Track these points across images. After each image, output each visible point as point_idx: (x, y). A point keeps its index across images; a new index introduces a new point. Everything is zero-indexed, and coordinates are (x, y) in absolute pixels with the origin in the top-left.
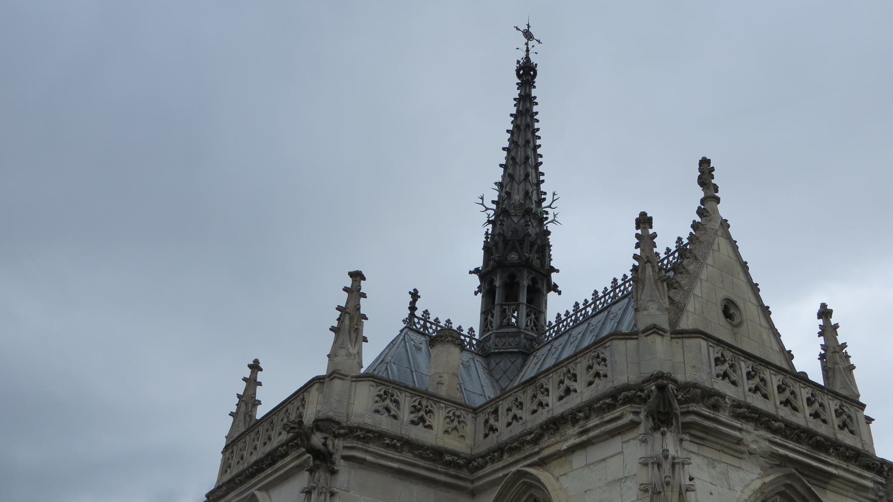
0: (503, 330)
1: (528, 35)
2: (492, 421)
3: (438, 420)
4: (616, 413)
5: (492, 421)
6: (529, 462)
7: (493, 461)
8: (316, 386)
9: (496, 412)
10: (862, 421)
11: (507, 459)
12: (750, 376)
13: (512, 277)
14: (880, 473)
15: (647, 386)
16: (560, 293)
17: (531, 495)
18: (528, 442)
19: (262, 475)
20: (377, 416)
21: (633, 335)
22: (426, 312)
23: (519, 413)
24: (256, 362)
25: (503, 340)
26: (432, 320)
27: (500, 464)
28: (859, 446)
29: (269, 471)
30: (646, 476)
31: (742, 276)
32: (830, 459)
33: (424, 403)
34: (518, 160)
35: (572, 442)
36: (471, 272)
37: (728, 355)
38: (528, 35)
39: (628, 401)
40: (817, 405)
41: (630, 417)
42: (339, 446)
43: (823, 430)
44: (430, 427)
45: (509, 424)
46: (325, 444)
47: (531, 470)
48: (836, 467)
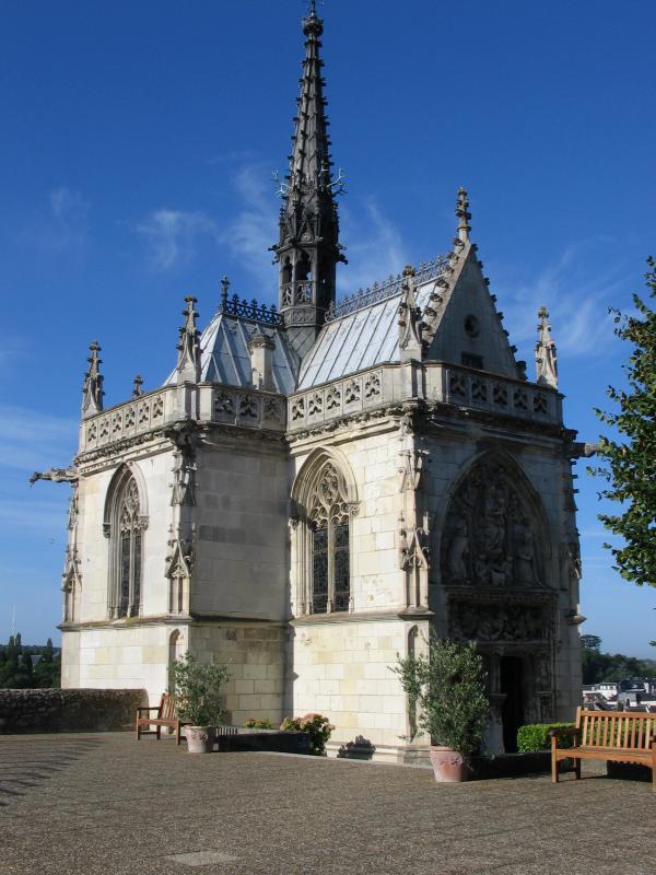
2: (298, 409)
3: (260, 411)
6: (327, 442)
9: (301, 401)
10: (554, 398)
11: (312, 438)
12: (474, 386)
14: (560, 437)
16: (346, 262)
17: (329, 463)
20: (219, 414)
22: (236, 296)
23: (319, 407)
25: (301, 315)
28: (548, 421)
33: (249, 399)
35: (356, 434)
36: (270, 250)
37: (460, 375)
40: (521, 398)
41: (392, 424)
43: (523, 415)
44: (254, 416)
45: (312, 413)
46: (186, 440)
47: (327, 448)
48: (529, 439)
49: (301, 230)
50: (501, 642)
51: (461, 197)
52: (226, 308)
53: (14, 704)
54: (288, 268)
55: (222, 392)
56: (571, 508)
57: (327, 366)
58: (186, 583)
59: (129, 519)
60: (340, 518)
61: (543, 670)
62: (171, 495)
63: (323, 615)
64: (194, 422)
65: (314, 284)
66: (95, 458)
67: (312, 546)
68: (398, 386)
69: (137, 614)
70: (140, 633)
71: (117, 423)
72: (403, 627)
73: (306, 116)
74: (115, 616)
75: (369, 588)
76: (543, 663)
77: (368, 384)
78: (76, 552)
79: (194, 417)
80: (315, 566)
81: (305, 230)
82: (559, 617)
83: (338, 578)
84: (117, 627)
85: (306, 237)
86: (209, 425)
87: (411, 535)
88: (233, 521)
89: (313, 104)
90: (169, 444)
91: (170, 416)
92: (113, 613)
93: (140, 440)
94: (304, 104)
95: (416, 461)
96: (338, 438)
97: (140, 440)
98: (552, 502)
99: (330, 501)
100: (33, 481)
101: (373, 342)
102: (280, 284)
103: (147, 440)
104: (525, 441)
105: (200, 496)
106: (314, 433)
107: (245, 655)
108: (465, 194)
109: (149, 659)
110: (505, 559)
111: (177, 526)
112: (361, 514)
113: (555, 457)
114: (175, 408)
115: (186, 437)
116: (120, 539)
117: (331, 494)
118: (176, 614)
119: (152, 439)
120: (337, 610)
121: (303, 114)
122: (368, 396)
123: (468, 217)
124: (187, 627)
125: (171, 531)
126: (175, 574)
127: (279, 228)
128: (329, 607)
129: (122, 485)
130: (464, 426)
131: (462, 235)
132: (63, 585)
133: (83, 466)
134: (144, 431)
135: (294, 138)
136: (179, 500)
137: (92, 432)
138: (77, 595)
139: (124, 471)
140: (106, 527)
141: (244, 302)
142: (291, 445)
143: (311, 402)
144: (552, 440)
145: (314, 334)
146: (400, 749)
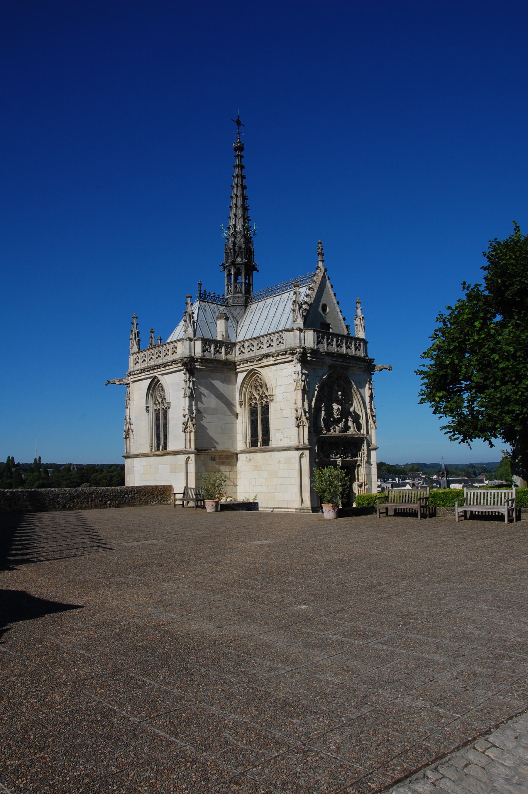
0: (237, 295)
1: (238, 123)
5: (242, 349)
7: (243, 364)
8: (181, 342)
9: (243, 346)
11: (249, 364)
13: (239, 269)
15: (296, 350)
16: (258, 271)
18: (257, 360)
19: (159, 370)
21: (292, 330)
22: (205, 291)
23: (252, 349)
25: (237, 299)
27: (246, 365)
29: (162, 369)
34: (238, 205)
38: (238, 123)
41: (290, 359)
45: (249, 352)
46: (190, 366)
49: (236, 256)
51: (320, 245)
52: (201, 297)
54: (229, 275)
55: (206, 342)
57: (253, 326)
58: (193, 435)
59: (159, 403)
60: (264, 402)
62: (184, 392)
63: (256, 448)
64: (193, 357)
65: (243, 284)
66: (140, 373)
67: (250, 415)
68: (292, 340)
69: (166, 449)
71: (151, 356)
72: (298, 453)
73: (236, 195)
74: (153, 450)
75: (279, 435)
77: (277, 339)
78: (130, 419)
79: (193, 355)
80: (251, 425)
81: (237, 257)
83: (263, 430)
84: (155, 456)
85: (239, 259)
86: (200, 359)
87: (300, 411)
89: (240, 189)
90: (182, 368)
91: (182, 354)
92: (152, 449)
93: (165, 365)
94: (235, 189)
95: (302, 376)
96: (263, 364)
97: (165, 365)
99: (258, 394)
100: (106, 385)
101: (276, 315)
102: (226, 283)
103: (169, 366)
104: (351, 365)
106: (250, 362)
108: (321, 244)
109: (173, 470)
111: (188, 408)
112: (275, 401)
113: (364, 372)
114: (184, 350)
115: (189, 364)
116: (154, 413)
117: (259, 390)
118: (188, 449)
119: (171, 365)
120: (263, 446)
121: (235, 194)
122: (278, 344)
123: (323, 255)
124: (194, 455)
125: (184, 410)
126: (186, 430)
127: (225, 254)
129: (155, 386)
130: (323, 359)
131: (320, 264)
132: (124, 436)
133: (132, 377)
134: (167, 361)
135: (231, 207)
136: (188, 395)
137: (137, 360)
139: (156, 380)
140: (147, 407)
141: (210, 293)
142: (238, 367)
143: (248, 346)
144: (363, 364)
145: (244, 309)
146: (296, 509)
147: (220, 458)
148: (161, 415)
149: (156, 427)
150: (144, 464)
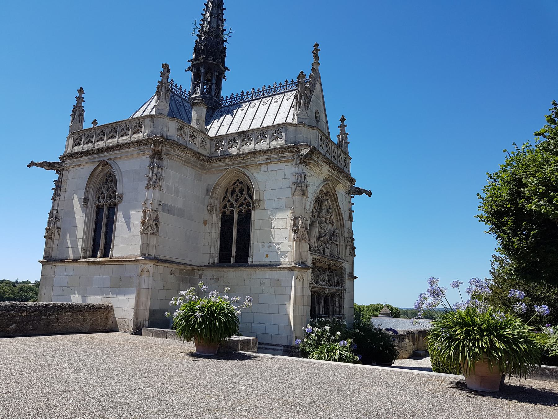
3: (198, 141)
4: (285, 155)
14: (351, 182)
24: (81, 88)
26: (174, 85)
30: (294, 179)
31: (322, 101)
32: (341, 177)
33: (194, 133)
39: (291, 151)
42: (164, 149)
50: (327, 287)
53: (25, 313)
56: (351, 219)
61: (337, 303)
70: (109, 268)
76: (337, 299)
82: (346, 277)
88: (179, 204)
93: (119, 147)
98: (345, 215)
99: (236, 201)
100: (29, 166)
105: (164, 184)
107: (179, 285)
110: (328, 242)
112: (262, 207)
114: (152, 129)
128: (232, 260)
133: (67, 162)
138: (56, 242)
146: (284, 346)
147: (181, 273)
148: (105, 211)
149: (94, 226)
150: (71, 274)
